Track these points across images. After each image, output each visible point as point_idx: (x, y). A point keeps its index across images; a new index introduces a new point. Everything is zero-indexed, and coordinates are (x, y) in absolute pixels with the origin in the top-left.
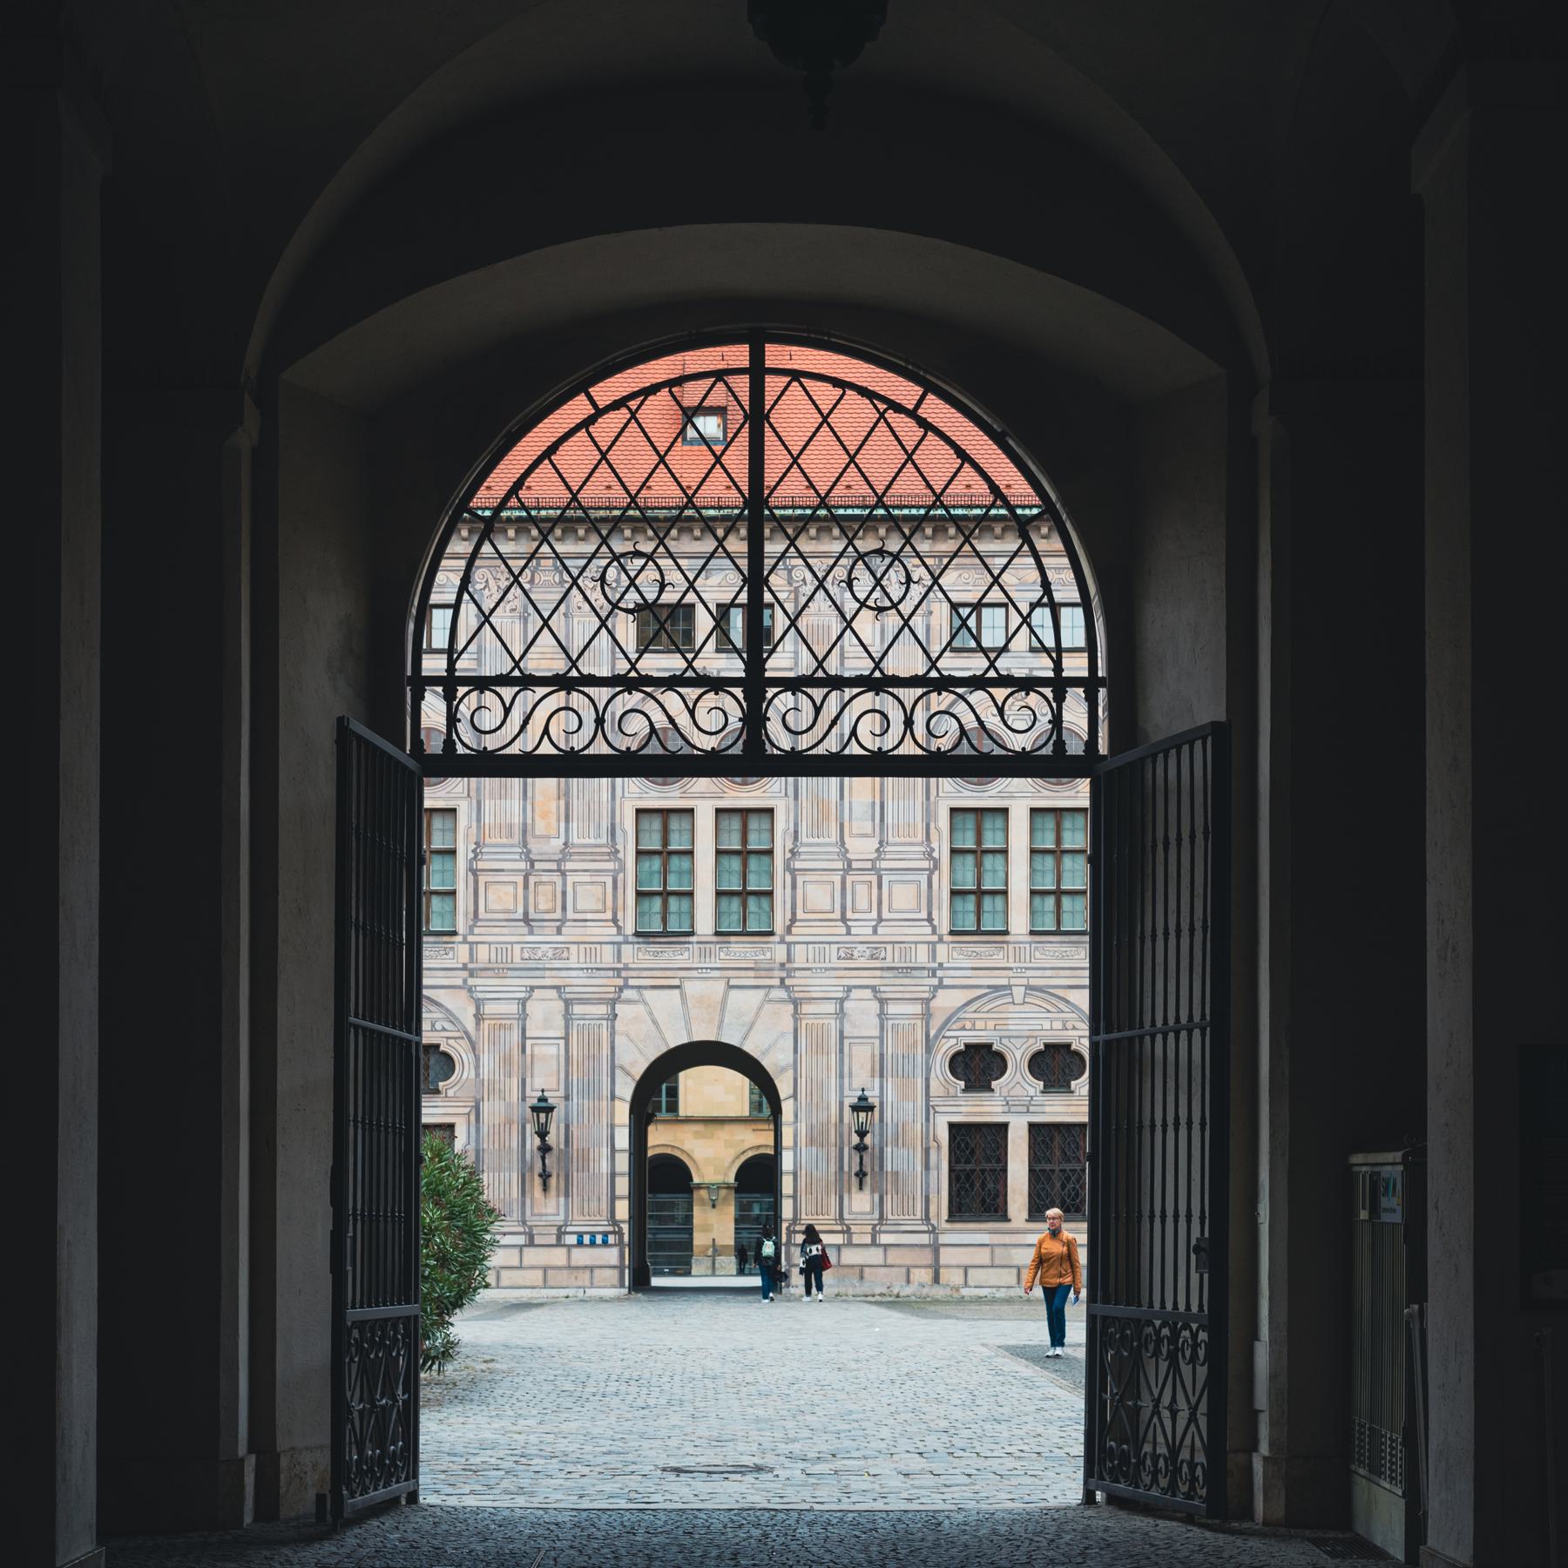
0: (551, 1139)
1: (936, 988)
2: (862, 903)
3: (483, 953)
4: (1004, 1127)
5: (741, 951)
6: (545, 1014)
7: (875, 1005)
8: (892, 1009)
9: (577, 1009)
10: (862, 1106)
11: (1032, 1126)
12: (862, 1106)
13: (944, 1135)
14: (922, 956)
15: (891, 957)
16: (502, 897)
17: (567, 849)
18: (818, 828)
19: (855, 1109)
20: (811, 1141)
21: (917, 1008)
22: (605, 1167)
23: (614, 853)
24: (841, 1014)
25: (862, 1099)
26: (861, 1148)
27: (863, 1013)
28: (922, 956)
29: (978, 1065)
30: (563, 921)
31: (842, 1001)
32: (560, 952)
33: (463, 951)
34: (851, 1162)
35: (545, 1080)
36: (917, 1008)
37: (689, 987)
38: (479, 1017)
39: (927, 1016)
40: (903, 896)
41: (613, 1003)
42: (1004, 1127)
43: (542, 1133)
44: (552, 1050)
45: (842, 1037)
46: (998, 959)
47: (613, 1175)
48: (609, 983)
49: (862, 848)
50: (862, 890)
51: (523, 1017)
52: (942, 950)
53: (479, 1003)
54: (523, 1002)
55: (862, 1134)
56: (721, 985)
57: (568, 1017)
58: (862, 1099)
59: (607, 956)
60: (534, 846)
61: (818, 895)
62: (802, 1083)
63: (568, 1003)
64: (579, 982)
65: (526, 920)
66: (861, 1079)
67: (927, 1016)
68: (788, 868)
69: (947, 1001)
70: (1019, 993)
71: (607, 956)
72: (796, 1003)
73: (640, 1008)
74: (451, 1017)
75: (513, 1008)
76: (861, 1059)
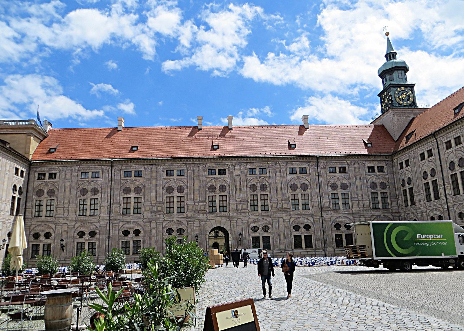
0: (198, 240)
1: (249, 219)
2: (239, 207)
3: (188, 215)
4: (259, 237)
5: (223, 214)
6: (197, 223)
7: (241, 221)
8: (243, 221)
9: (201, 223)
10: (240, 234)
11: (263, 237)
12: (240, 234)
13: (251, 238)
14: (247, 214)
15: (243, 214)
16: (191, 208)
17: (199, 202)
18: (233, 198)
19: (239, 235)
20: (233, 240)
21: (247, 221)
22: (205, 244)
23: (206, 202)
24: (237, 222)
25: (240, 234)
26: (240, 240)
27: (239, 221)
28: (247, 214)
29: (255, 229)
30: (199, 211)
31: (237, 221)
32: (199, 215)
33: (186, 215)
34: (239, 243)
35: (197, 232)
36: (247, 221)
37: (216, 219)
38: (188, 224)
39: (248, 222)
40: (244, 206)
41: (206, 221)
42: (259, 237)
43: (197, 240)
44: (198, 228)
45: (237, 225)
46: (257, 214)
47: (206, 245)
48: (205, 219)
49: (238, 200)
50: (239, 206)
51: (194, 224)
52: (250, 213)
53: (188, 222)
54: (194, 222)
55: (240, 238)
56: (220, 219)
57: (200, 224)
58: (240, 234)
59: (205, 215)
60: (195, 201)
61: (233, 207)
62: (232, 232)
63: (200, 222)
64: (201, 219)
65: (194, 211)
66: (240, 231)
67: (248, 222)
68: (229, 203)
69: (251, 220)
70: (260, 219)
71: (205, 215)
72: (231, 221)
73: (209, 222)
74: (184, 224)
75: (192, 223)
76: (239, 228)
